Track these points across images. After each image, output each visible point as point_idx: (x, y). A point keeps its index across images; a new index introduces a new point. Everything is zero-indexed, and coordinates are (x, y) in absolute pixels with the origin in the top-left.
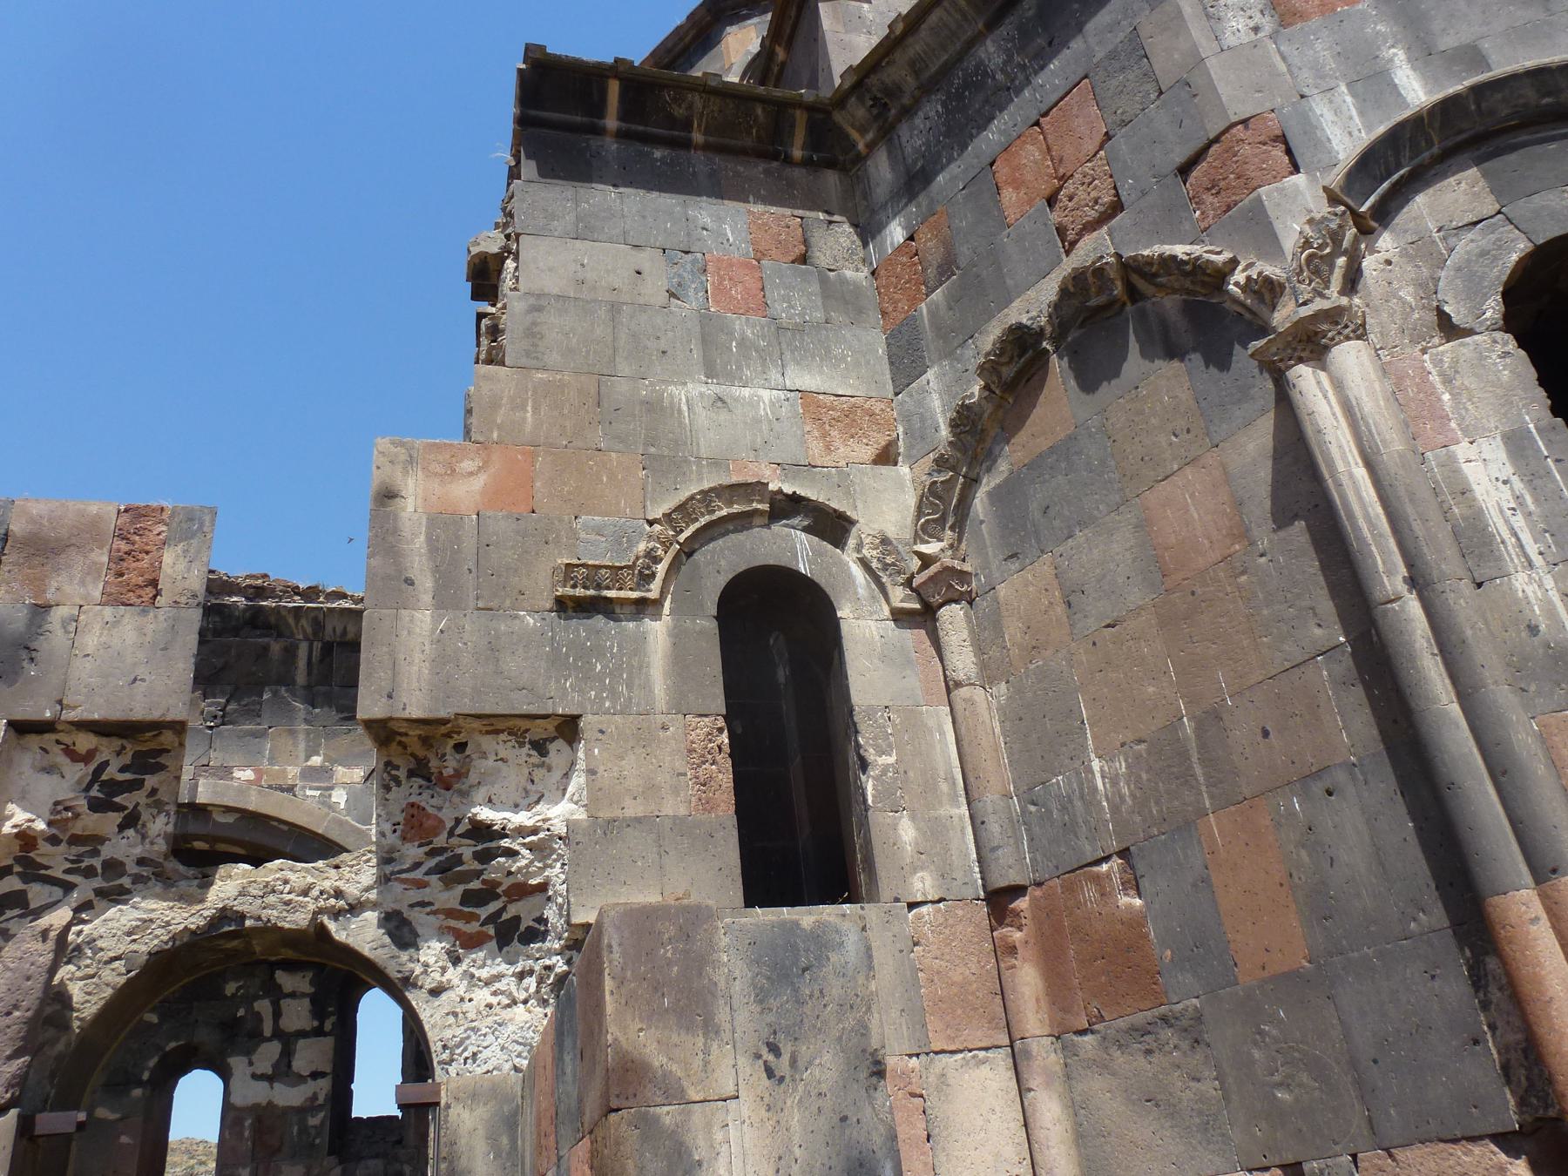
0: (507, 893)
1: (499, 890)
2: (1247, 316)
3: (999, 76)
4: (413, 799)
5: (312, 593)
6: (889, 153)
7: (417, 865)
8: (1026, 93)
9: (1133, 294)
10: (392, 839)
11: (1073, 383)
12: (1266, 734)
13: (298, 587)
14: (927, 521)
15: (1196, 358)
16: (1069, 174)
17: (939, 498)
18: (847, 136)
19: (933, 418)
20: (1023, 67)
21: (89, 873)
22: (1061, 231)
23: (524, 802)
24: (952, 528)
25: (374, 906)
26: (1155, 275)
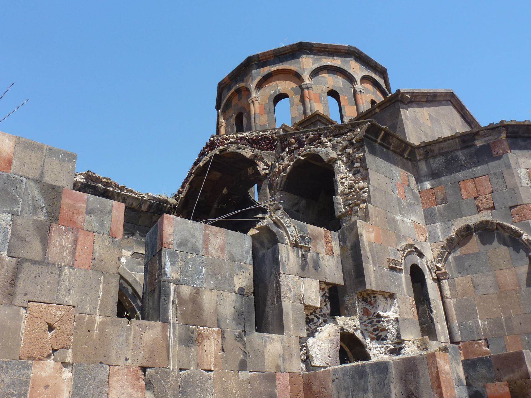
0: (381, 330)
1: (379, 329)
2: (524, 244)
3: (462, 162)
4: (365, 306)
5: (122, 188)
6: (426, 164)
7: (365, 322)
8: (471, 170)
9: (497, 227)
10: (361, 315)
11: (479, 241)
12: (521, 324)
13: (118, 185)
14: (439, 259)
15: (511, 248)
16: (481, 195)
17: (442, 255)
18: (416, 155)
19: (438, 234)
20: (470, 164)
21: (322, 315)
22: (478, 207)
23: (384, 311)
24: (443, 262)
25: (359, 329)
26: (505, 229)
